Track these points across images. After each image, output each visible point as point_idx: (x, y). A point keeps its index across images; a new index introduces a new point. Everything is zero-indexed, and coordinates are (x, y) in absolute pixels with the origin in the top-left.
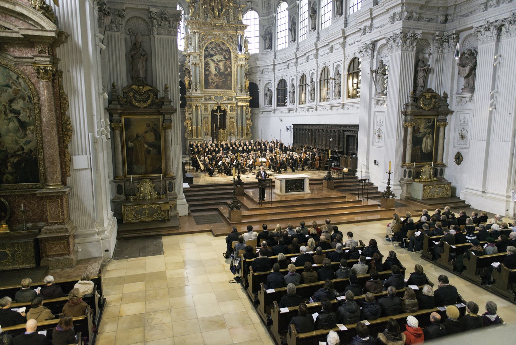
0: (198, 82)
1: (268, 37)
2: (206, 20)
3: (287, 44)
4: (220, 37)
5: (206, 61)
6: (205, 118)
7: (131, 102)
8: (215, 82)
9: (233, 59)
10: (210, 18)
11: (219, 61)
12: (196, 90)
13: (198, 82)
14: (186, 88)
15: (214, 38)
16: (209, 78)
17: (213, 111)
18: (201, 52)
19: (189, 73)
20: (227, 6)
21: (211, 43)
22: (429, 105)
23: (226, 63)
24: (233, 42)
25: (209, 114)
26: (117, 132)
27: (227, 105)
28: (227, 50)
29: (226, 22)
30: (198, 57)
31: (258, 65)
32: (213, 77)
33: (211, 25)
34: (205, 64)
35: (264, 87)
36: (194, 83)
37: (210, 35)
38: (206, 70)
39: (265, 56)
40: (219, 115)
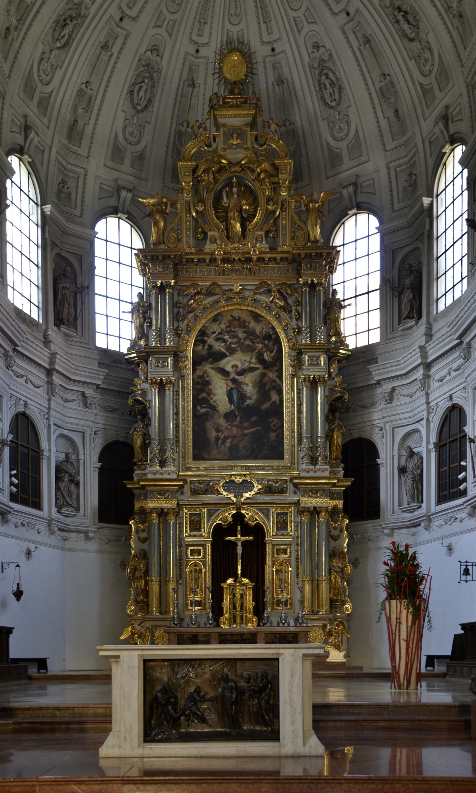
4: (244, 298)
5: (199, 372)
6: (193, 552)
8: (226, 438)
9: (286, 361)
10: (215, 242)
11: (242, 373)
12: (163, 464)
14: (135, 460)
15: (227, 300)
16: (209, 424)
20: (269, 200)
21: (215, 319)
23: (263, 375)
24: (286, 309)
28: (267, 337)
29: (264, 246)
31: (376, 378)
32: (222, 422)
33: (215, 260)
34: (195, 383)
35: (396, 447)
36: (155, 443)
37: (209, 293)
40: (239, 544)
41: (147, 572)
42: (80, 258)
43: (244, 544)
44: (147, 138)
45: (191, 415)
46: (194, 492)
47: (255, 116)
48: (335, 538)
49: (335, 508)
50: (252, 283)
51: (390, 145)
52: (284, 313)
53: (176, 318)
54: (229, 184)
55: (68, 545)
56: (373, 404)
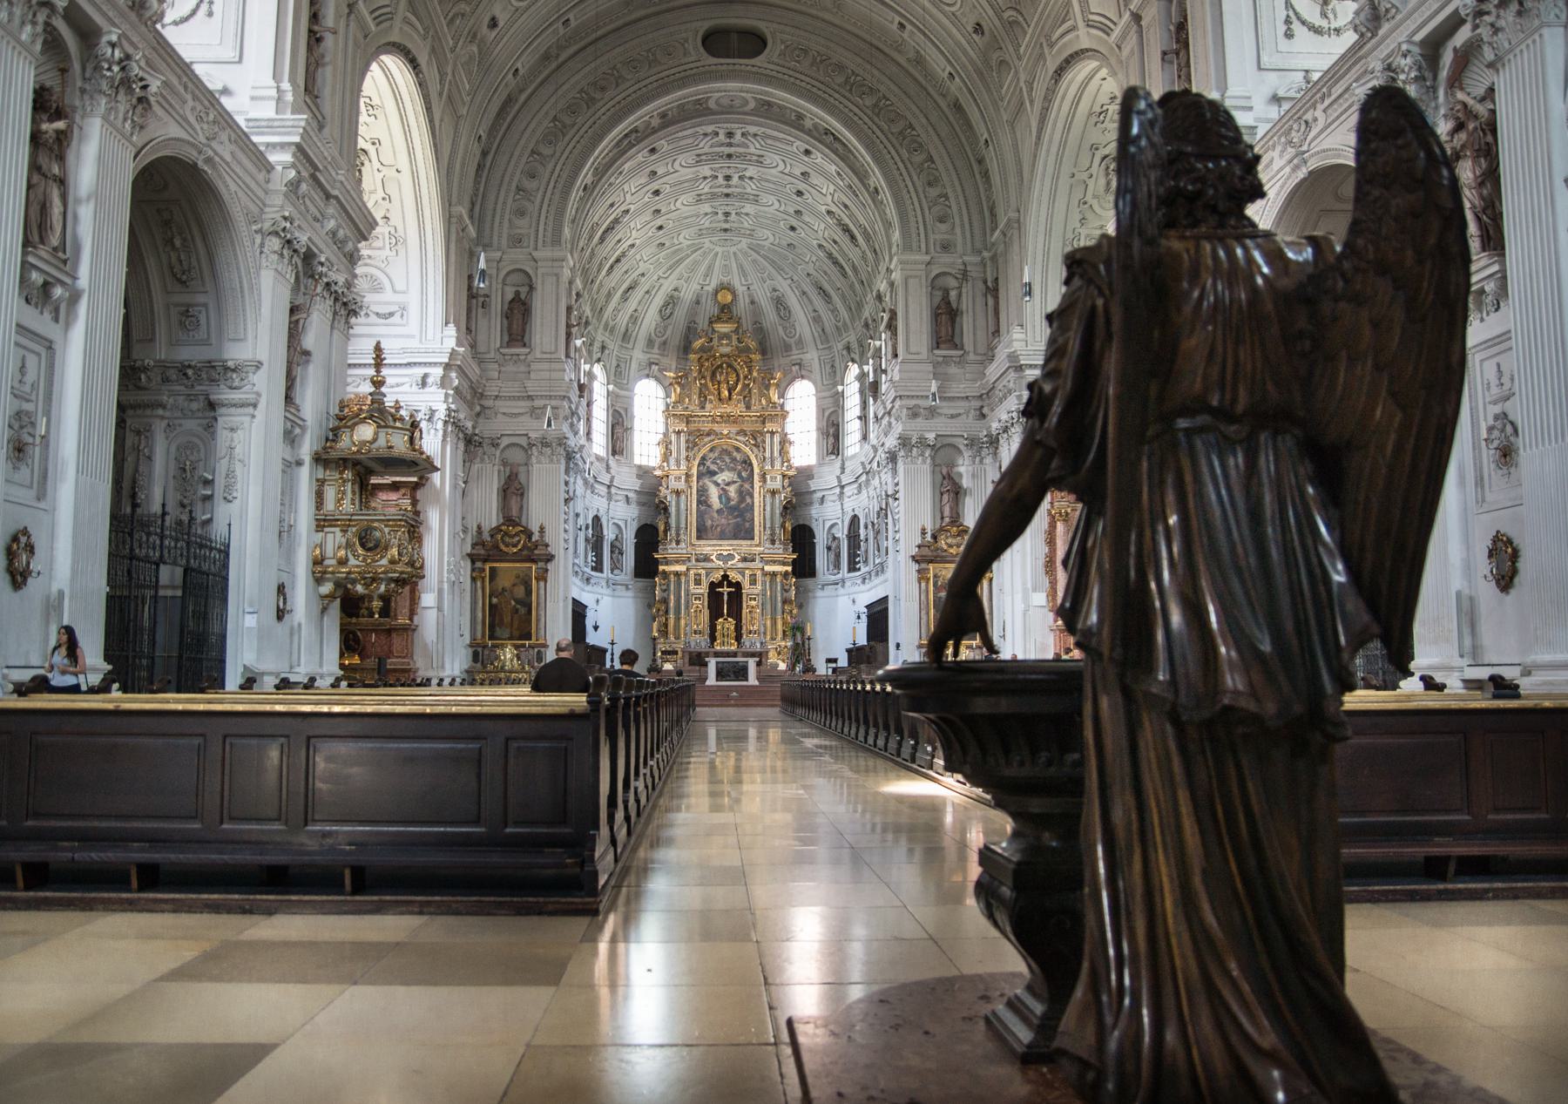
0: (683, 525)
1: (831, 431)
2: (703, 408)
3: (858, 445)
7: (497, 547)
11: (728, 484)
13: (683, 525)
17: (712, 586)
18: (689, 468)
19: (666, 509)
21: (711, 450)
22: (958, 546)
24: (756, 445)
25: (703, 589)
26: (479, 584)
27: (742, 572)
28: (745, 462)
29: (742, 406)
30: (683, 478)
32: (715, 515)
37: (708, 434)
38: (699, 502)
39: (826, 469)
41: (667, 612)
42: (626, 410)
43: (729, 593)
44: (669, 332)
45: (694, 511)
46: (697, 560)
47: (736, 331)
48: (786, 591)
49: (786, 573)
50: (734, 429)
51: (820, 347)
52: (755, 449)
53: (687, 448)
54: (720, 366)
55: (616, 593)
56: (811, 503)
